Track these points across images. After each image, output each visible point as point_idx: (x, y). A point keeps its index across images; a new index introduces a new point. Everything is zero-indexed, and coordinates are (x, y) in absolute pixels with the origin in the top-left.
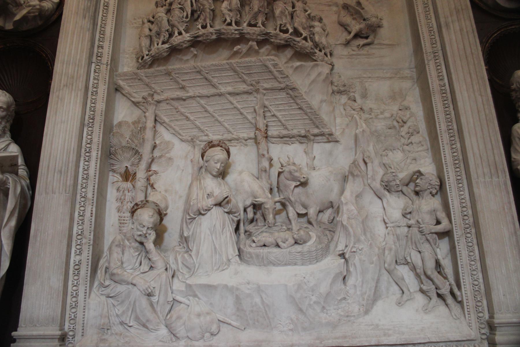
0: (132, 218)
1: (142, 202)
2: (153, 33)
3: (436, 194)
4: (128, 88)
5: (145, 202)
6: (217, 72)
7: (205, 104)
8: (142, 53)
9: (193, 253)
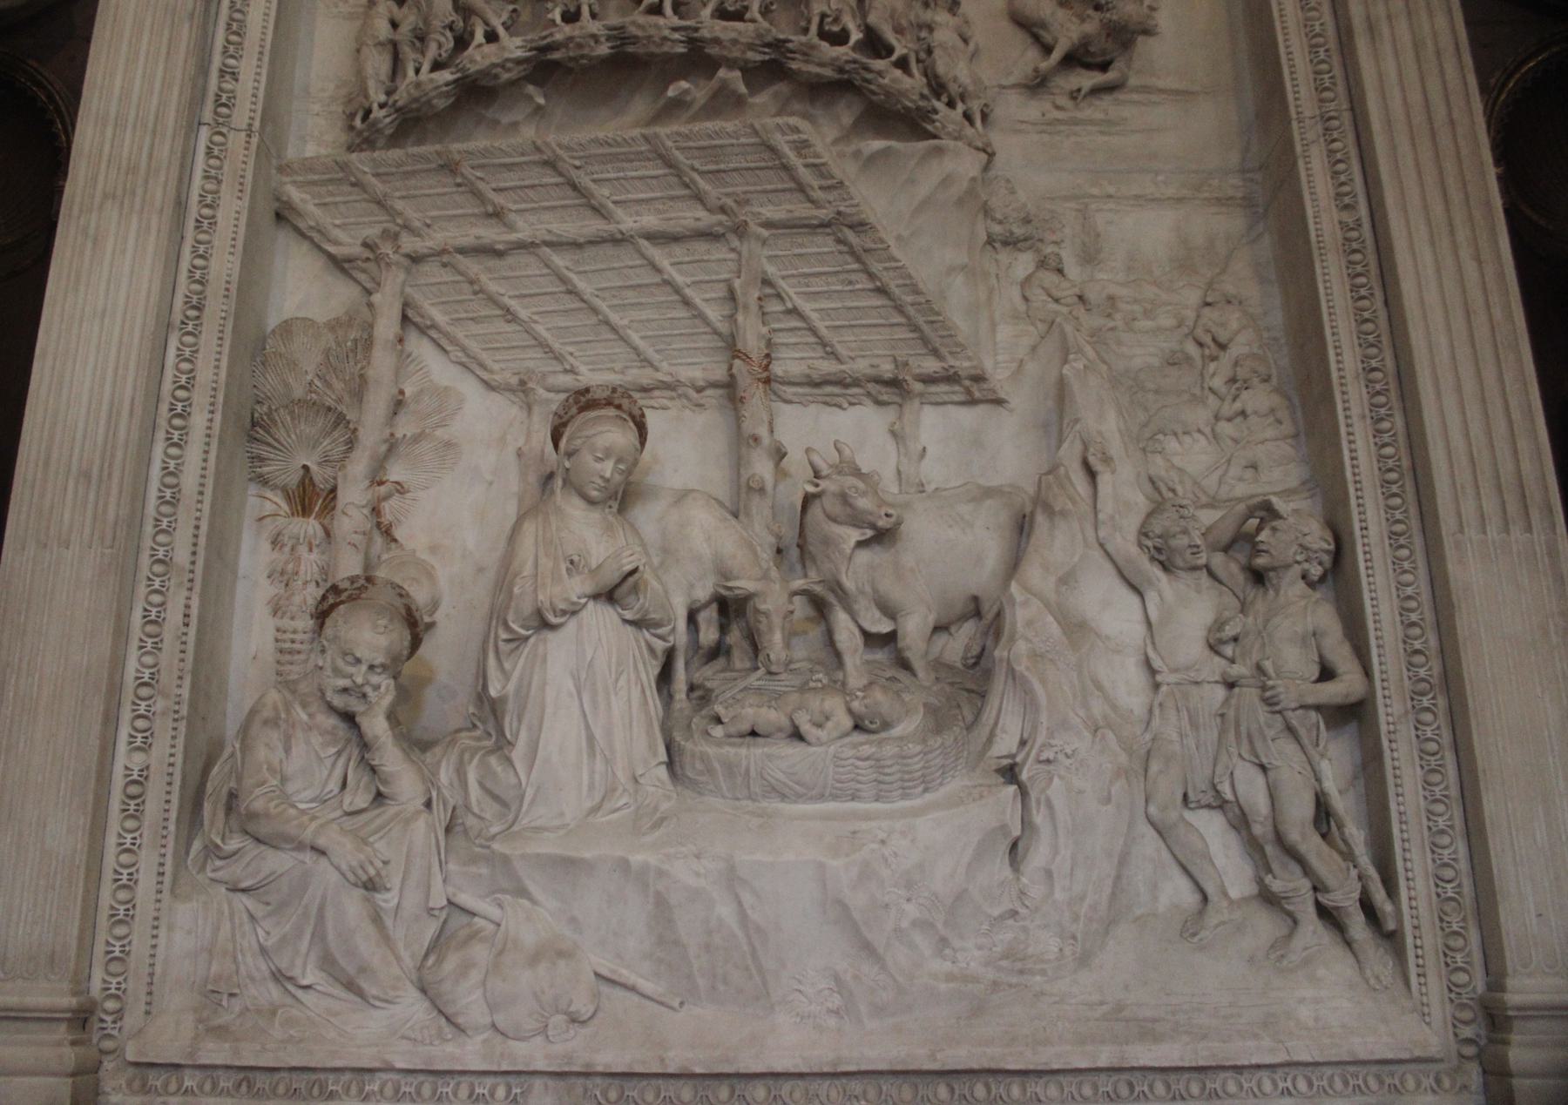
0: (320, 635)
1: (352, 583)
3: (1322, 579)
4: (317, 212)
5: (362, 582)
6: (609, 166)
7: (567, 268)
8: (366, 96)
9: (518, 754)
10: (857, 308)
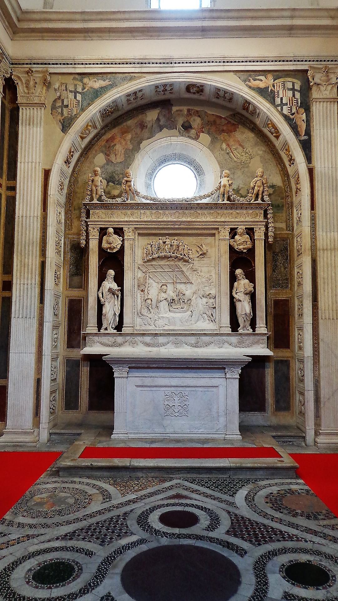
2: (148, 253)
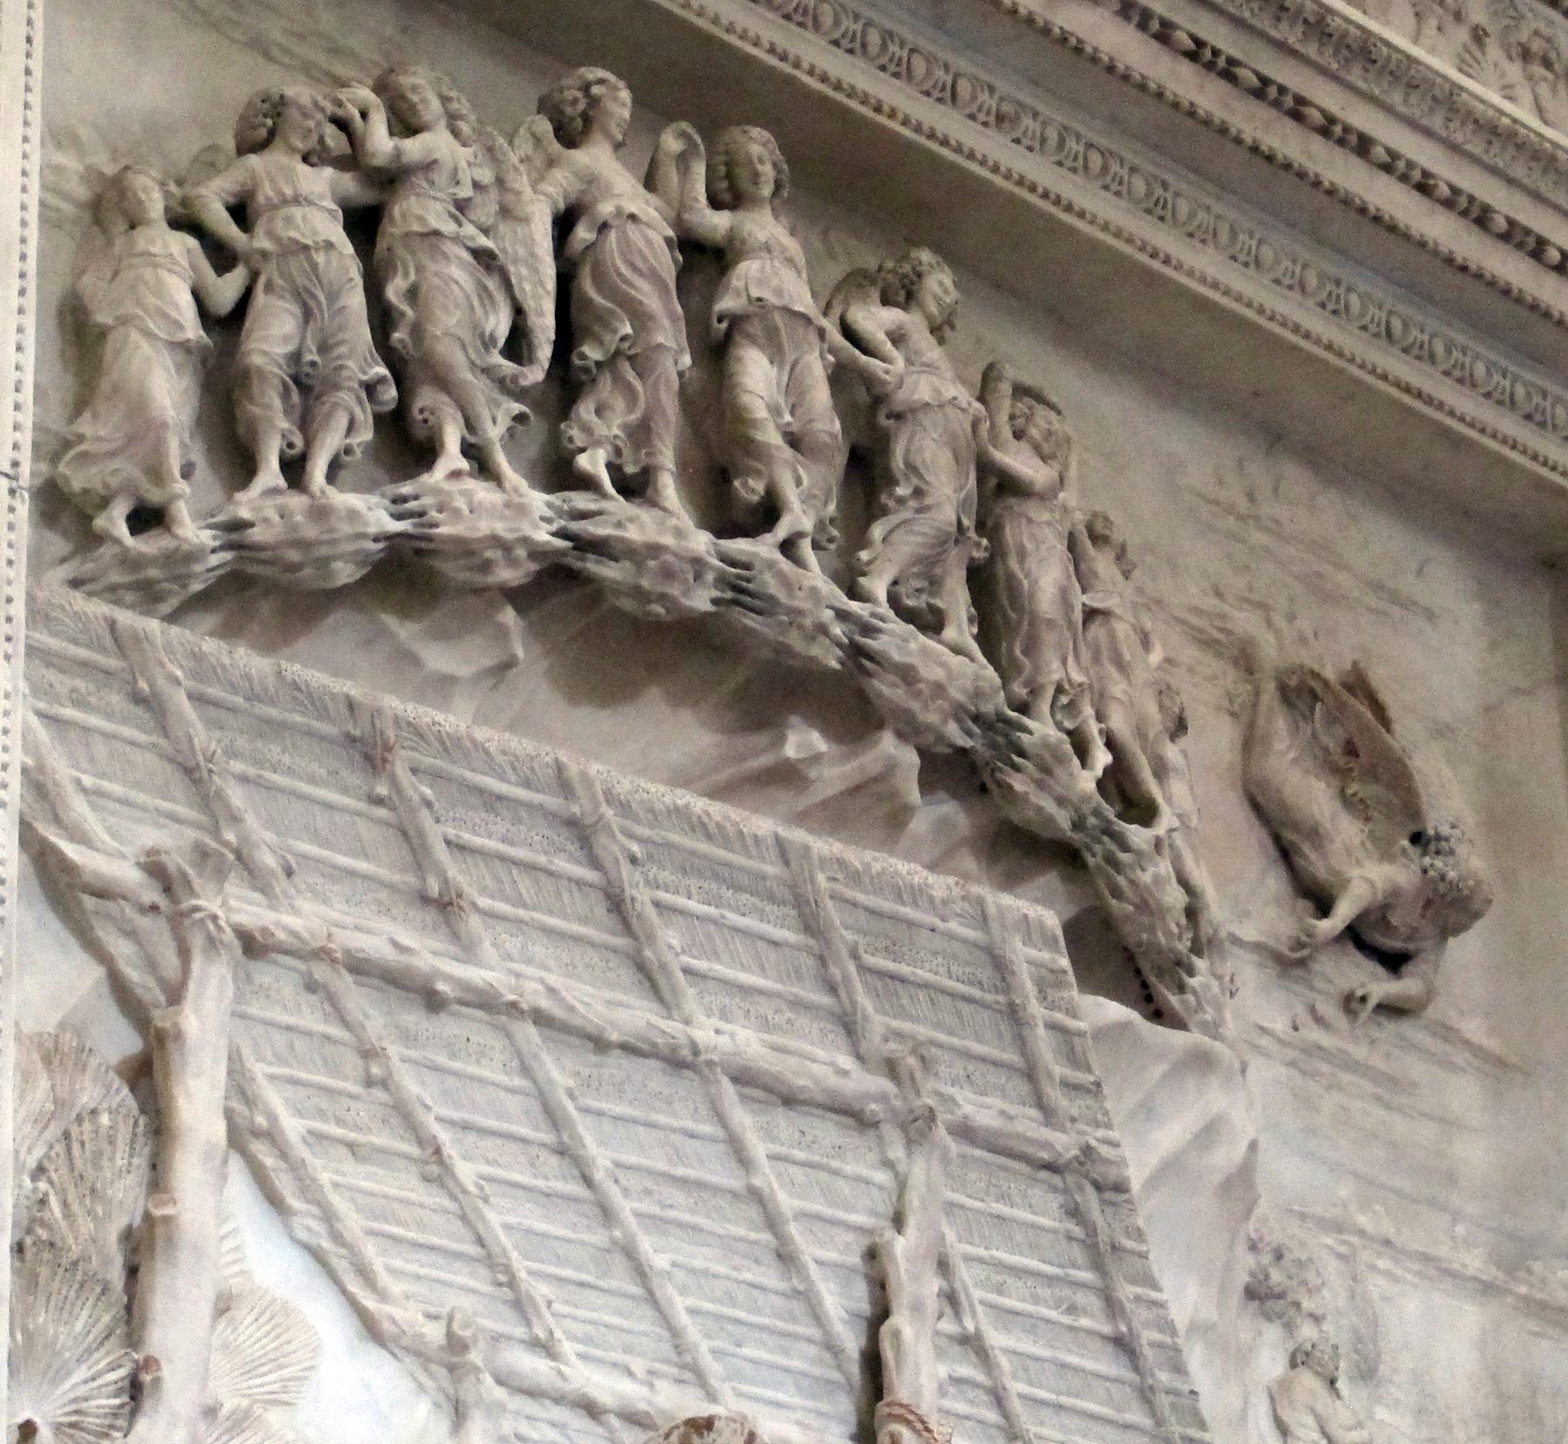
6: (693, 883)
10: (1077, 1370)
